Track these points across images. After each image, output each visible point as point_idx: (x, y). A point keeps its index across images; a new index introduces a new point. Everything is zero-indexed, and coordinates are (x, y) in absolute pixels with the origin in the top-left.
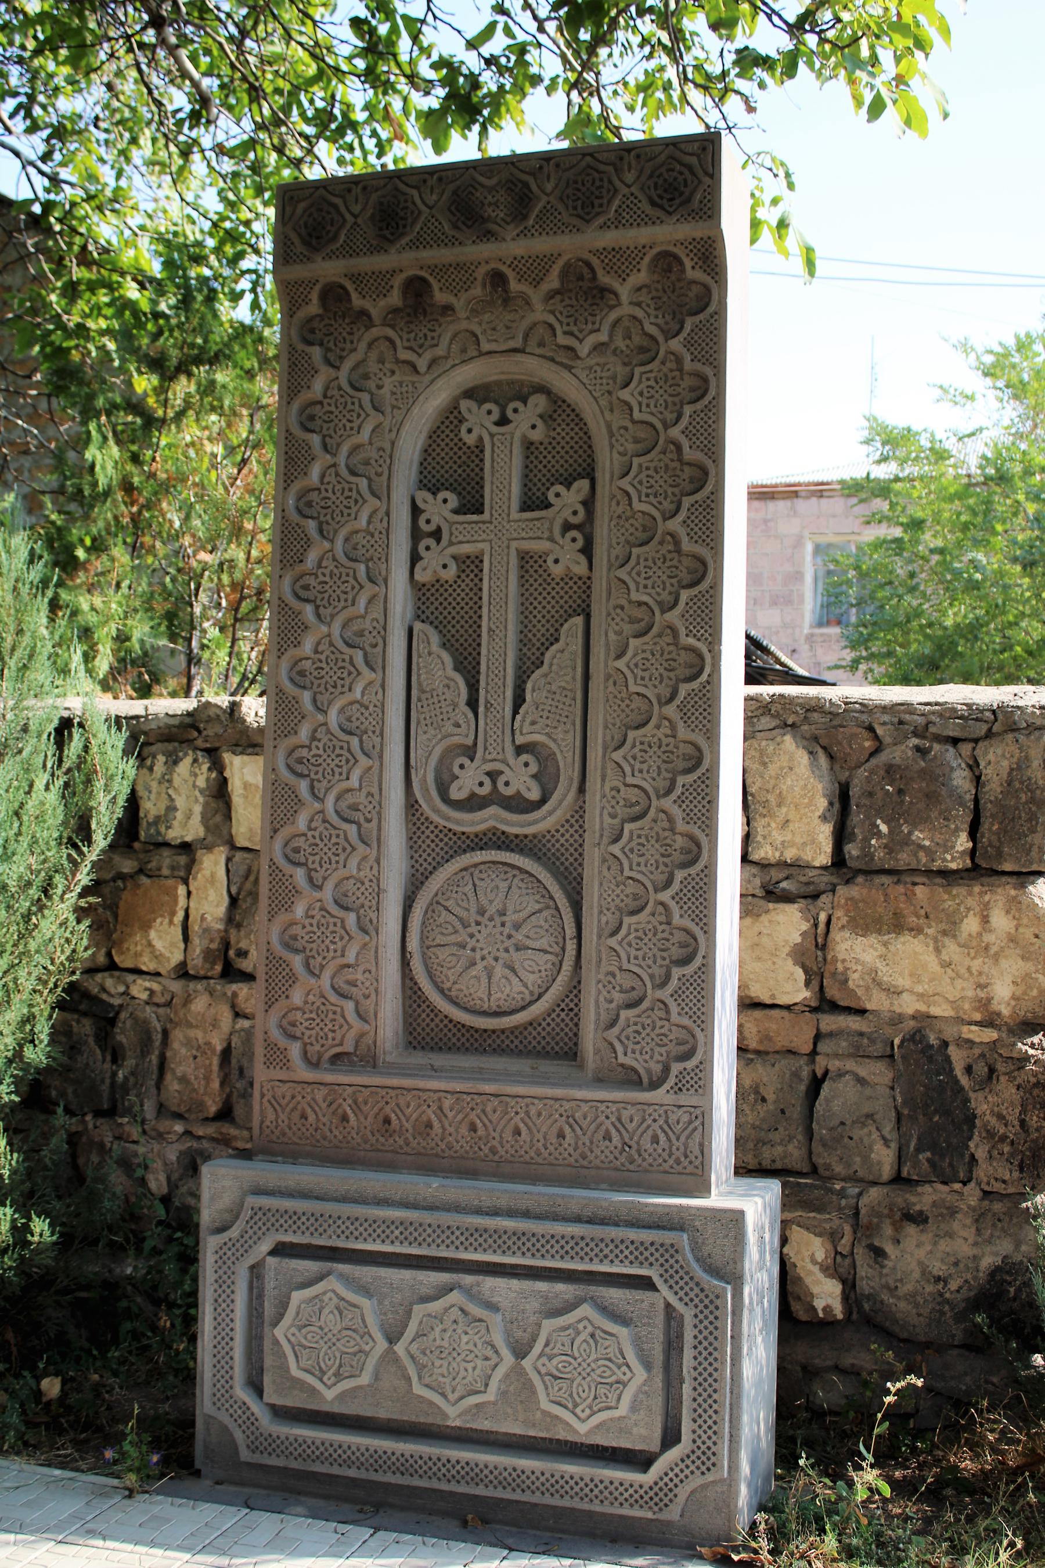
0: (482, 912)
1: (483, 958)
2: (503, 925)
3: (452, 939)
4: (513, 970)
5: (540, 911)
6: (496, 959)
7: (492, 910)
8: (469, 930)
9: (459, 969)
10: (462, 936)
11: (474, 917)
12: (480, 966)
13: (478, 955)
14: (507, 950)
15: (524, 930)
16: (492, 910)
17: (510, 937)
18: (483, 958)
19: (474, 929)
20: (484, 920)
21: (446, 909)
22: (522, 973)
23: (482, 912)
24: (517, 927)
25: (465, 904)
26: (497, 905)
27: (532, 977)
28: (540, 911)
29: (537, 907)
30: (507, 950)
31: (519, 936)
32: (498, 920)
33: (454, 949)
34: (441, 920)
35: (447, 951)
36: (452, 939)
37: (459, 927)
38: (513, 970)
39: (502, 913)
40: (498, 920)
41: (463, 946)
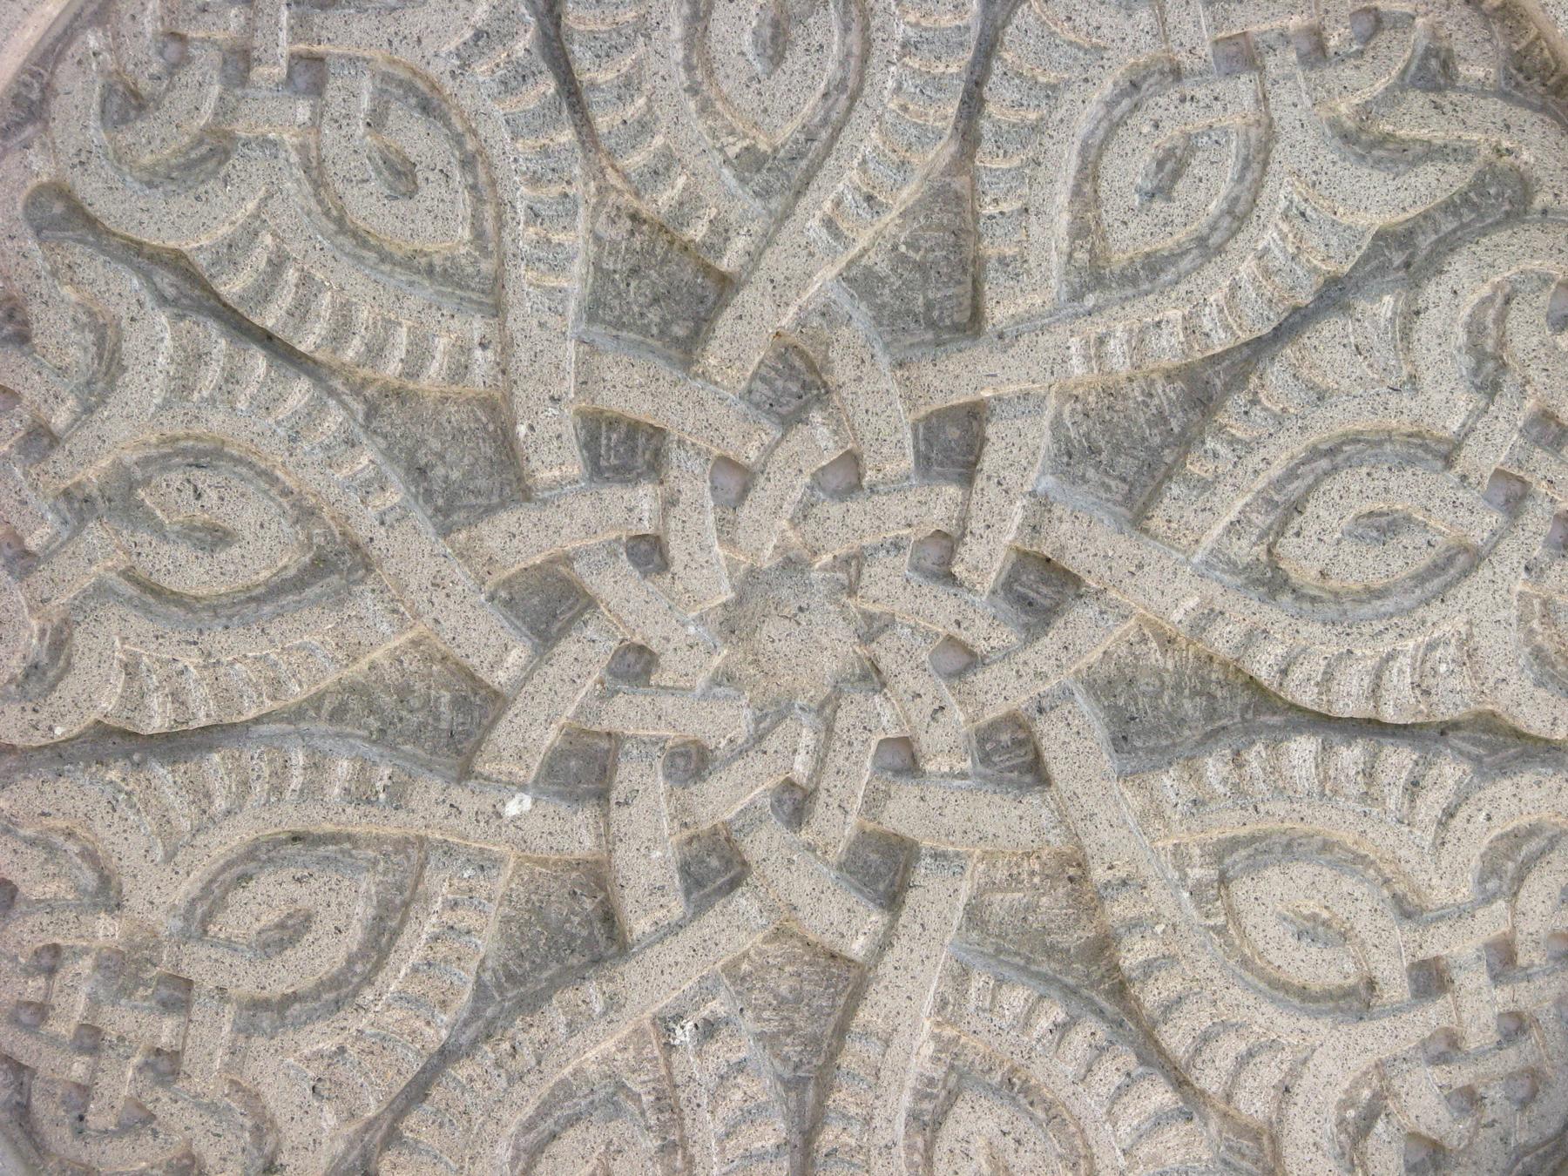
0: (671, 292)
1: (715, 869)
2: (955, 443)
3: (310, 651)
4: (1100, 983)
5: (1405, 256)
6: (885, 870)
7: (798, 275)
8: (515, 541)
9: (402, 1015)
10: (437, 599)
11: (558, 371)
12: (677, 962)
13: (647, 839)
14: (1014, 755)
15: (1215, 510)
16: (798, 275)
17: (1042, 588)
18: (715, 869)
19: (574, 520)
20: (703, 410)
21: (191, 288)
22: (1197, 1000)
23: (671, 292)
24: (1140, 450)
25: (440, 224)
26: (864, 203)
27: (1338, 1059)
28: (1405, 256)
29: (1378, 202)
30: (1014, 755)
31: (1163, 585)
32: (882, 403)
33: (333, 784)
34: (123, 432)
35: (236, 803)
36: (310, 651)
37: (381, 510)
38: (1100, 983)
39: (940, 292)
40: (882, 403)
41: (451, 724)
